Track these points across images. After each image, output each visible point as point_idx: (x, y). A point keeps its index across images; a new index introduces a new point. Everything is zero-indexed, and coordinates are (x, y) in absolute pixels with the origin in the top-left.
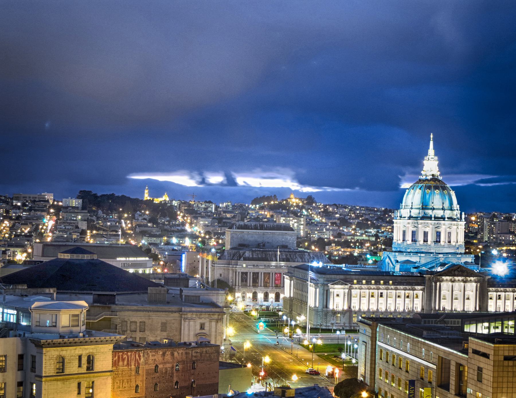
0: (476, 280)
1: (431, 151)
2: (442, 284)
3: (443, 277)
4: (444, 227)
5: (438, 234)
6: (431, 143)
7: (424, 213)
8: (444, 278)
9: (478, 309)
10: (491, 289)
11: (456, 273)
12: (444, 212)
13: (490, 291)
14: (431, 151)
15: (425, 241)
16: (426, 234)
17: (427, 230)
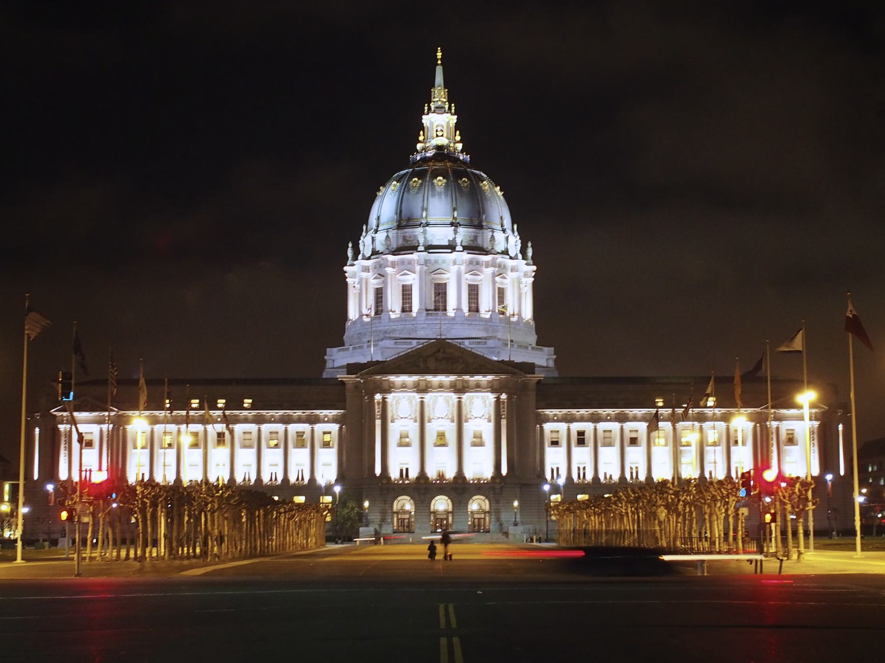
0: (496, 385)
1: (439, 95)
2: (390, 397)
3: (392, 378)
4: (454, 269)
5: (440, 291)
6: (439, 71)
7: (404, 238)
8: (398, 379)
9: (504, 471)
10: (548, 412)
11: (432, 364)
12: (456, 232)
13: (547, 420)
14: (439, 95)
15: (406, 309)
16: (406, 292)
17: (412, 279)
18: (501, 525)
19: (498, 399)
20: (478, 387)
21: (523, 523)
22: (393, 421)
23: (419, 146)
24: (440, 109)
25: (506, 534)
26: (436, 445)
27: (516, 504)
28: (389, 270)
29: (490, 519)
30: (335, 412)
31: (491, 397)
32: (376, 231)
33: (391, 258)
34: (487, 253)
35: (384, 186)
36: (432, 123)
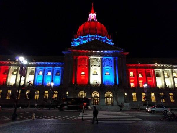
1: (93, 10)
10: (130, 65)
14: (93, 10)
18: (118, 102)
19: (115, 59)
20: (108, 55)
21: (128, 103)
22: (79, 66)
23: (88, 20)
24: (93, 13)
25: (121, 106)
26: (93, 74)
27: (126, 94)
28: (81, 40)
29: (113, 100)
30: (61, 63)
31: (111, 58)
32: (78, 34)
33: (82, 37)
34: (103, 37)
35: (81, 26)
36: (91, 15)
